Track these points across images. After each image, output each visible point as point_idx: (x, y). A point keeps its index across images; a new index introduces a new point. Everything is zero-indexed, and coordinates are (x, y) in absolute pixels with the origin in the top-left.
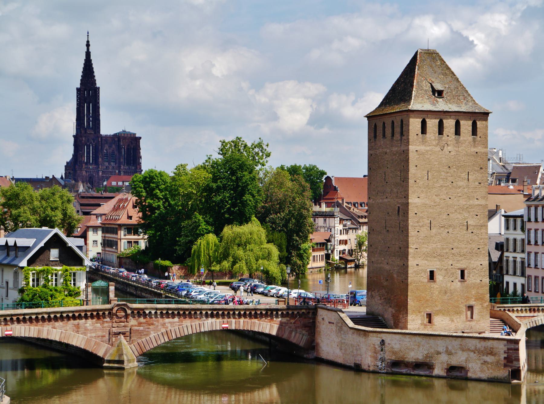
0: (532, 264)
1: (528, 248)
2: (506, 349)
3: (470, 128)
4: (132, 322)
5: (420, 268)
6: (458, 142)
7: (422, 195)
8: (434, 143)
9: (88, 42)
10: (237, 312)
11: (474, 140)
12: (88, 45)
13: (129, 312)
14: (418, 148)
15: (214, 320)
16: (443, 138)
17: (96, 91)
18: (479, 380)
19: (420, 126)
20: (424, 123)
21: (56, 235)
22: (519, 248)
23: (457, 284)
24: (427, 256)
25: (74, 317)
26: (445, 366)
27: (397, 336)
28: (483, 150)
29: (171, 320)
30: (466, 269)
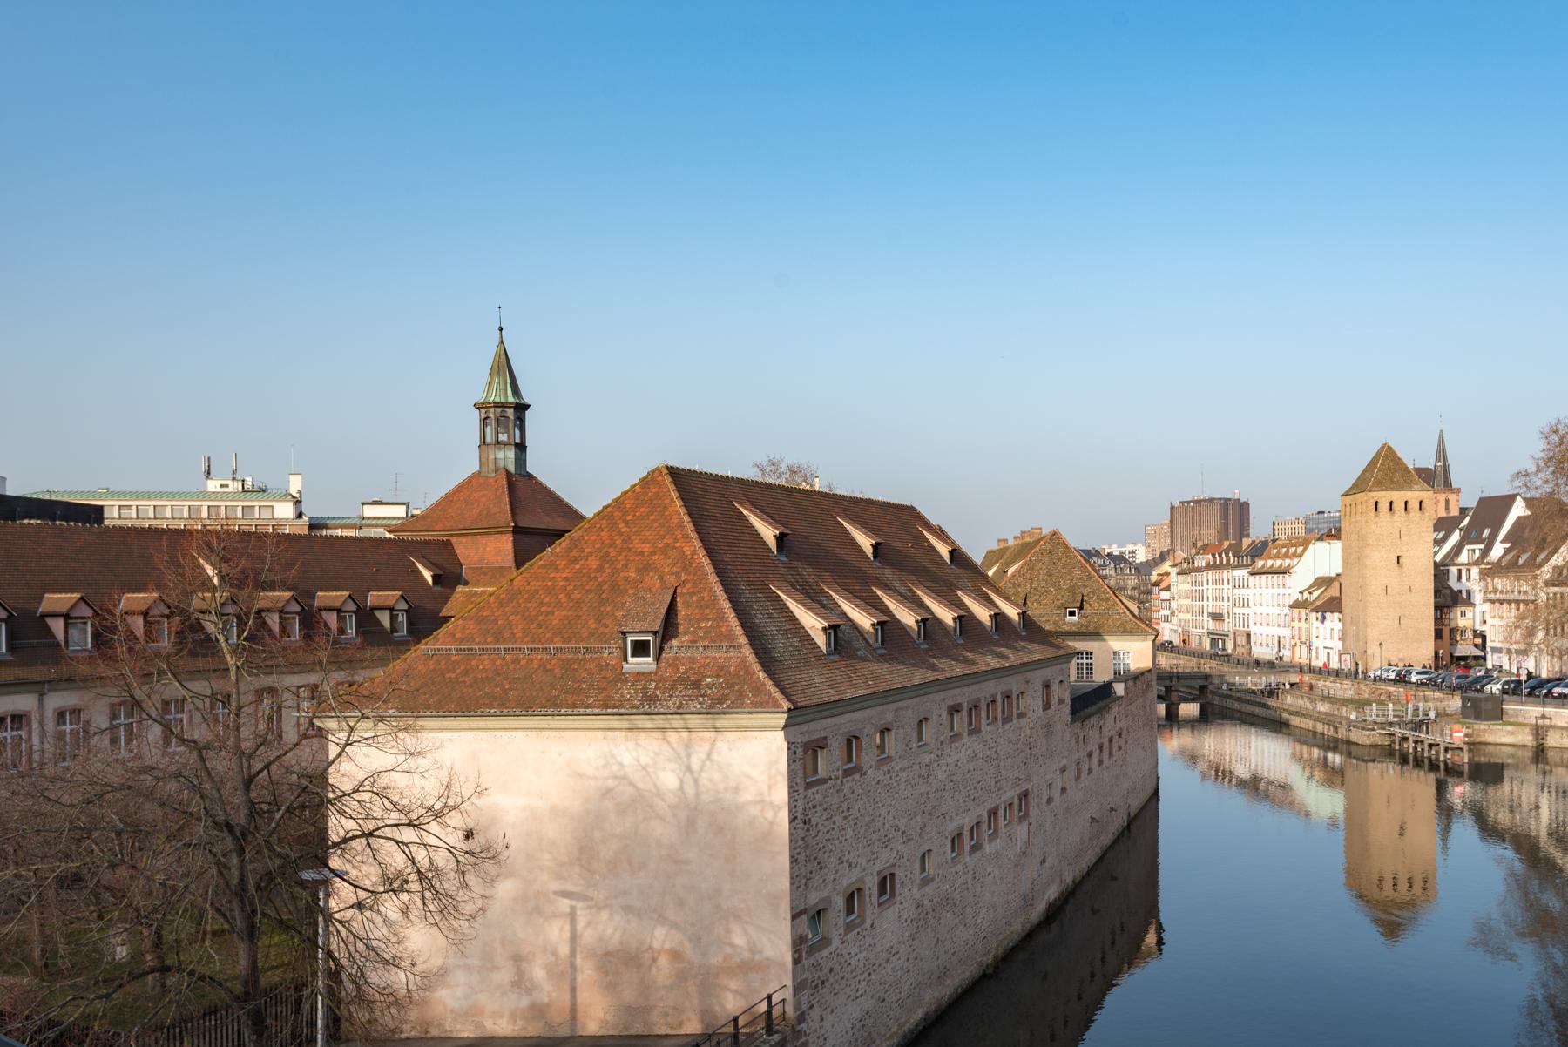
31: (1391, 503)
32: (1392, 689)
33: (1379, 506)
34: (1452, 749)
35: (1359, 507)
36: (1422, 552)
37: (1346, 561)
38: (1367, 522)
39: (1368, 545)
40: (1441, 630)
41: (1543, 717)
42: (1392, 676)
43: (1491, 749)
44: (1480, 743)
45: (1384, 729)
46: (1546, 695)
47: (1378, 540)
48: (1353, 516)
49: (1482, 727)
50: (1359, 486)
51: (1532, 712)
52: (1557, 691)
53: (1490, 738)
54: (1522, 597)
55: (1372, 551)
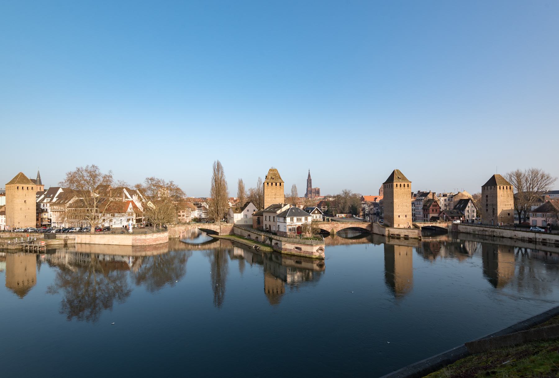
0: (417, 214)
1: (416, 211)
4: (335, 225)
6: (404, 188)
17: (311, 179)
18: (412, 238)
19: (396, 185)
20: (397, 184)
21: (317, 208)
22: (413, 210)
23: (405, 218)
26: (404, 235)
31: (23, 187)
32: (22, 234)
33: (19, 188)
34: (41, 247)
35: (12, 188)
36: (32, 200)
37: (7, 202)
38: (14, 192)
39: (15, 198)
40: (38, 219)
41: (67, 237)
42: (23, 231)
43: (52, 245)
44: (49, 245)
45: (20, 244)
46: (67, 232)
47: (18, 196)
48: (10, 190)
49: (50, 241)
50: (12, 182)
51: (64, 236)
52: (70, 231)
53: (52, 243)
54: (61, 210)
55: (16, 199)
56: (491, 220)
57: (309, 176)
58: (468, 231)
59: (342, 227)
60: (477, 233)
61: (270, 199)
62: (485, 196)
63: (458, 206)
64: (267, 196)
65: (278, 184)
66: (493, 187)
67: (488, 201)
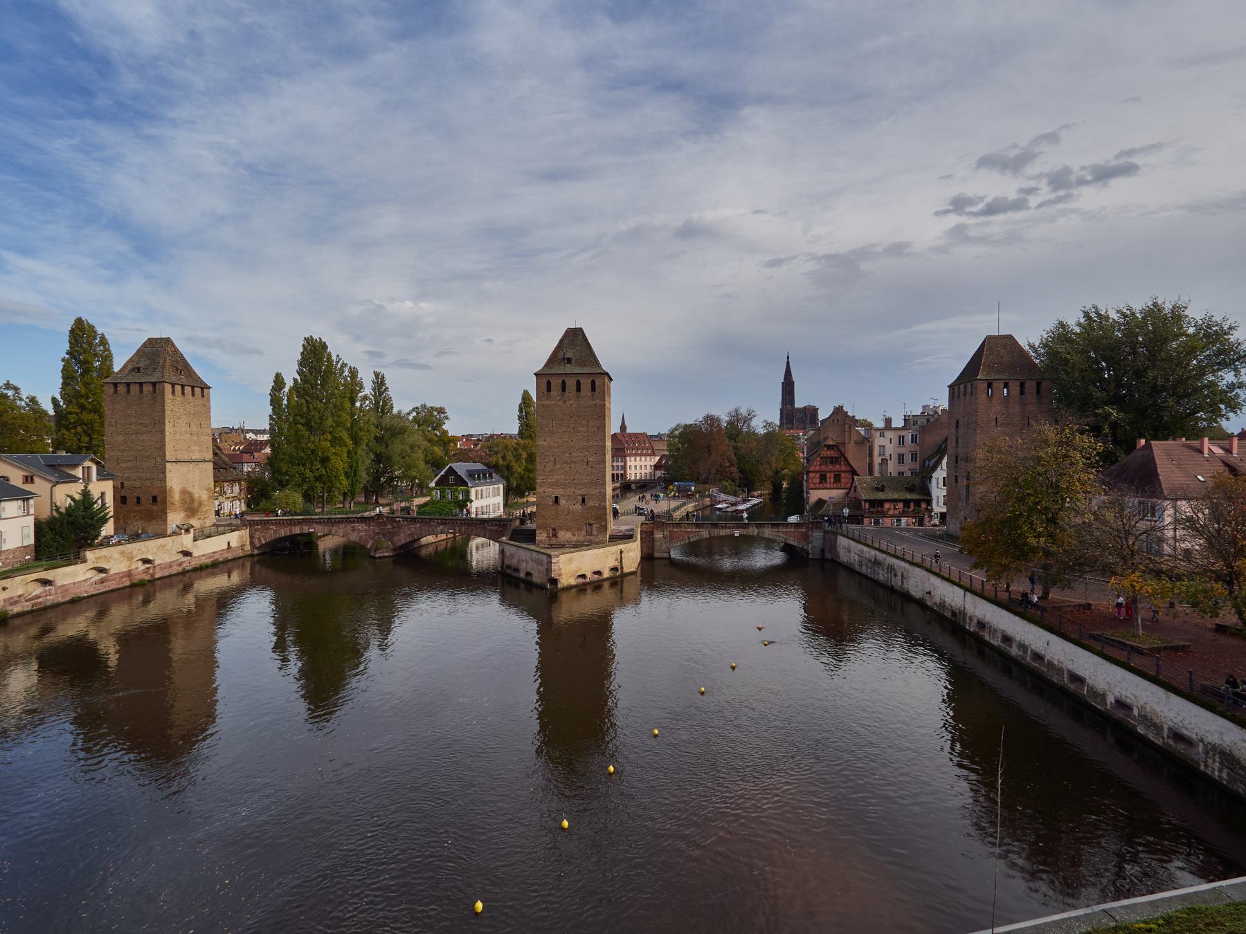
2: (546, 562)
3: (590, 386)
5: (546, 494)
7: (548, 439)
8: (557, 398)
9: (788, 356)
10: (459, 522)
11: (593, 395)
12: (788, 358)
13: (385, 519)
14: (544, 403)
15: (442, 527)
16: (566, 394)
19: (545, 386)
20: (549, 383)
21: (451, 467)
23: (578, 507)
24: (552, 485)
25: (351, 522)
27: (508, 546)
28: (602, 402)
29: (414, 526)
30: (585, 495)
56: (963, 518)
57: (788, 373)
58: (852, 561)
59: (411, 535)
60: (864, 570)
61: (121, 438)
62: (955, 422)
63: (927, 463)
64: (112, 426)
65: (147, 388)
66: (969, 386)
67: (959, 444)
